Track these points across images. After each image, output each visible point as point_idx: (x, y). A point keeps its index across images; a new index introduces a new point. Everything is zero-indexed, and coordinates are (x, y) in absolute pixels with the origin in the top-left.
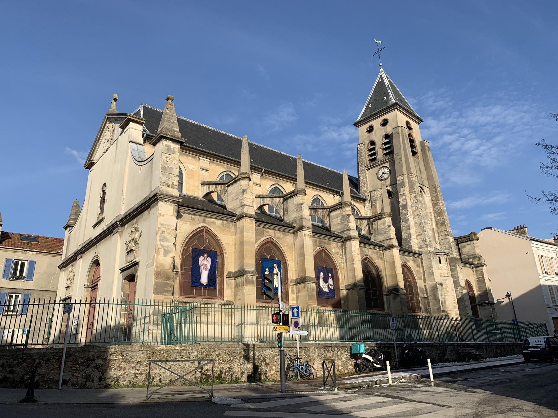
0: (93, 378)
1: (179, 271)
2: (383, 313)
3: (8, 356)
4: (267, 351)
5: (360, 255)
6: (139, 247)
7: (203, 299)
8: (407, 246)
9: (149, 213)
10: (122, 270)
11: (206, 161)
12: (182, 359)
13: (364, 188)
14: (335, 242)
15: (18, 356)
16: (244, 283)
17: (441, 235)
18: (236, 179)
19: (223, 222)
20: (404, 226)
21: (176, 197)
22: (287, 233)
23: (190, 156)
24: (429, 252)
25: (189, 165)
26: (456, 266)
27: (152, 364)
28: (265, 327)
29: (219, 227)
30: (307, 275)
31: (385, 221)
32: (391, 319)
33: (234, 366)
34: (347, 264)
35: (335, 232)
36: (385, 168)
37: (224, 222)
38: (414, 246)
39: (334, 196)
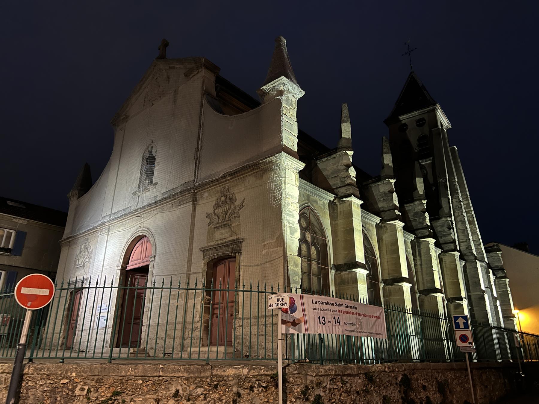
3: (187, 379)
10: (204, 251)
15: (204, 379)
34: (423, 266)
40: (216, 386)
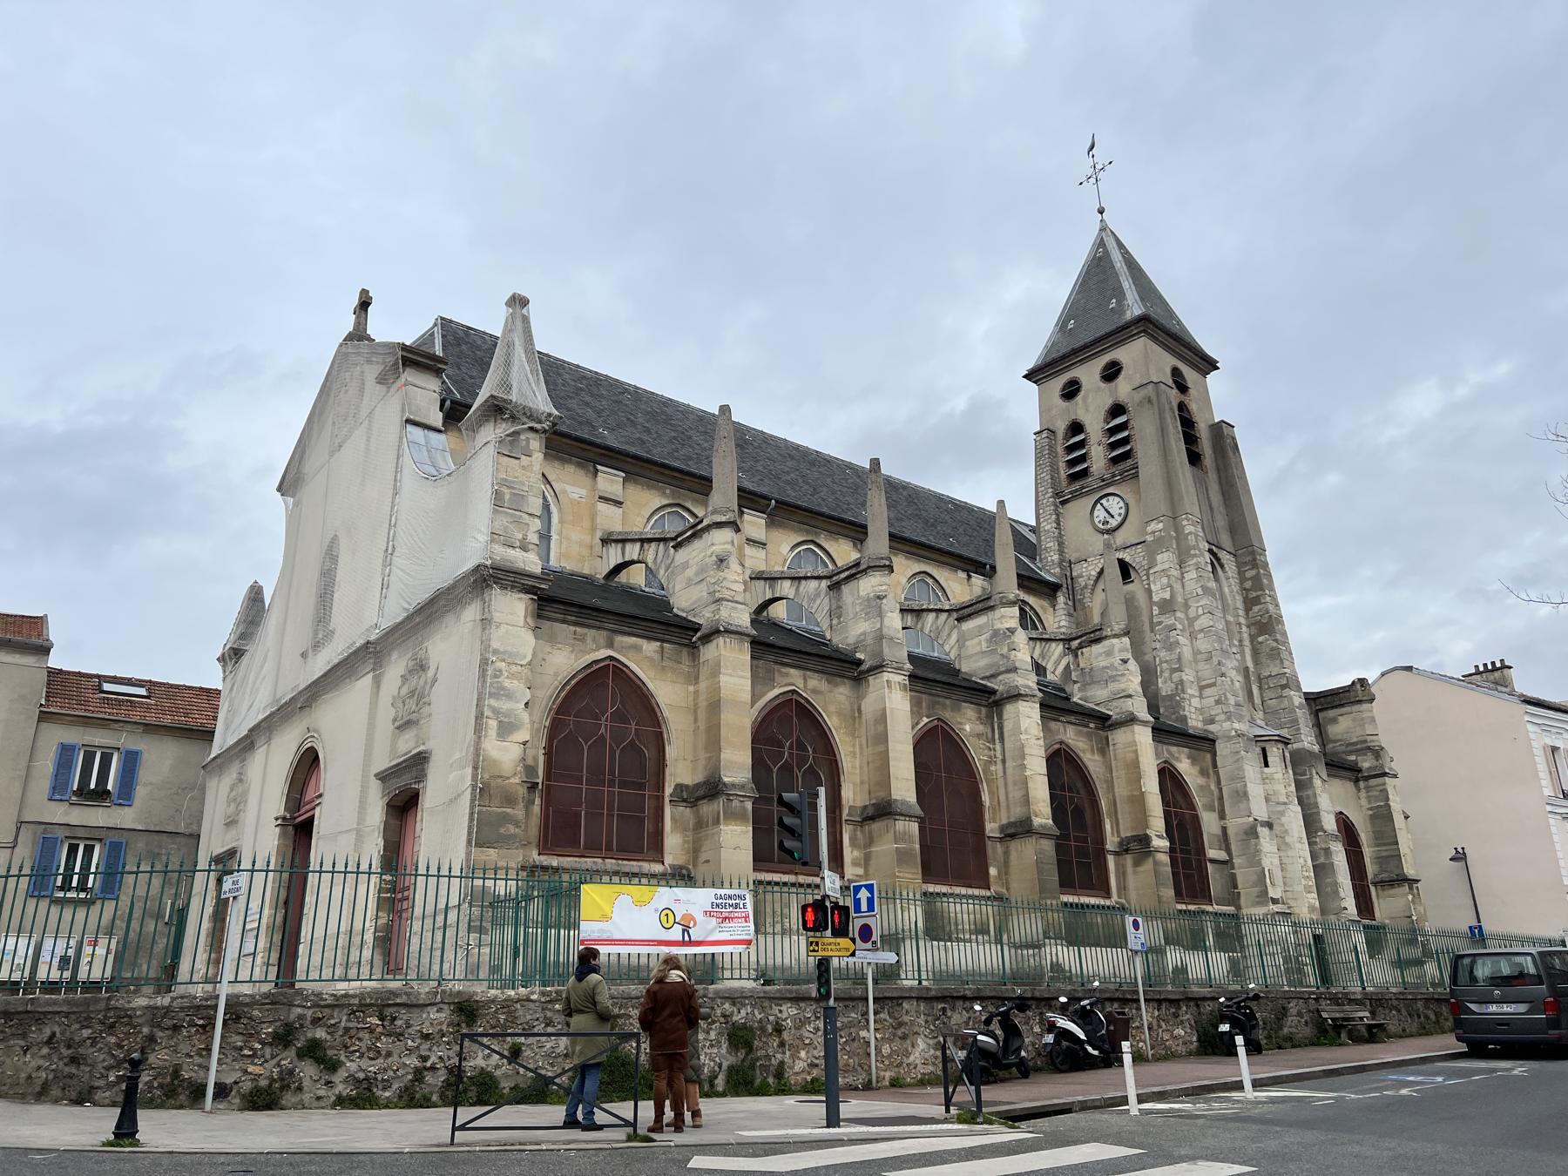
0: (301, 1078)
1: (540, 781)
2: (1108, 903)
3: (67, 1015)
4: (784, 1008)
5: (1041, 742)
6: (430, 715)
7: (607, 860)
8: (1174, 717)
9: (458, 618)
10: (383, 777)
11: (615, 475)
12: (550, 1030)
13: (1052, 554)
14: (972, 703)
17: (1269, 688)
18: (699, 527)
19: (662, 647)
20: (1166, 662)
21: (531, 576)
22: (839, 679)
23: (570, 462)
24: (1233, 733)
25: (569, 488)
26: (1311, 774)
27: (467, 1043)
28: (778, 938)
29: (650, 659)
30: (894, 797)
31: (1113, 645)
32: (1129, 920)
34: (1007, 765)
36: (1111, 498)
38: (1194, 716)
39: (969, 577)
40: (112, 1026)
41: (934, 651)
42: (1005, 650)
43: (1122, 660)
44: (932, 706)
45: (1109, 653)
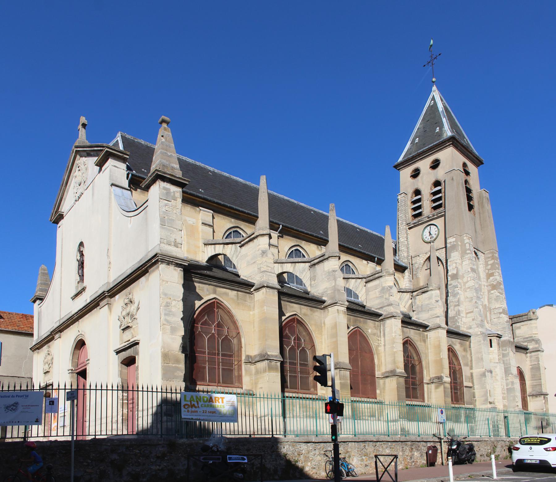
1: (188, 353)
4: (302, 446)
5: (401, 337)
13: (404, 253)
14: (372, 320)
16: (266, 369)
22: (315, 309)
31: (432, 294)
33: (266, 461)
35: (371, 308)
37: (239, 293)
39: (368, 263)
41: (352, 297)
42: (387, 296)
43: (436, 301)
44: (355, 321)
45: (430, 298)
